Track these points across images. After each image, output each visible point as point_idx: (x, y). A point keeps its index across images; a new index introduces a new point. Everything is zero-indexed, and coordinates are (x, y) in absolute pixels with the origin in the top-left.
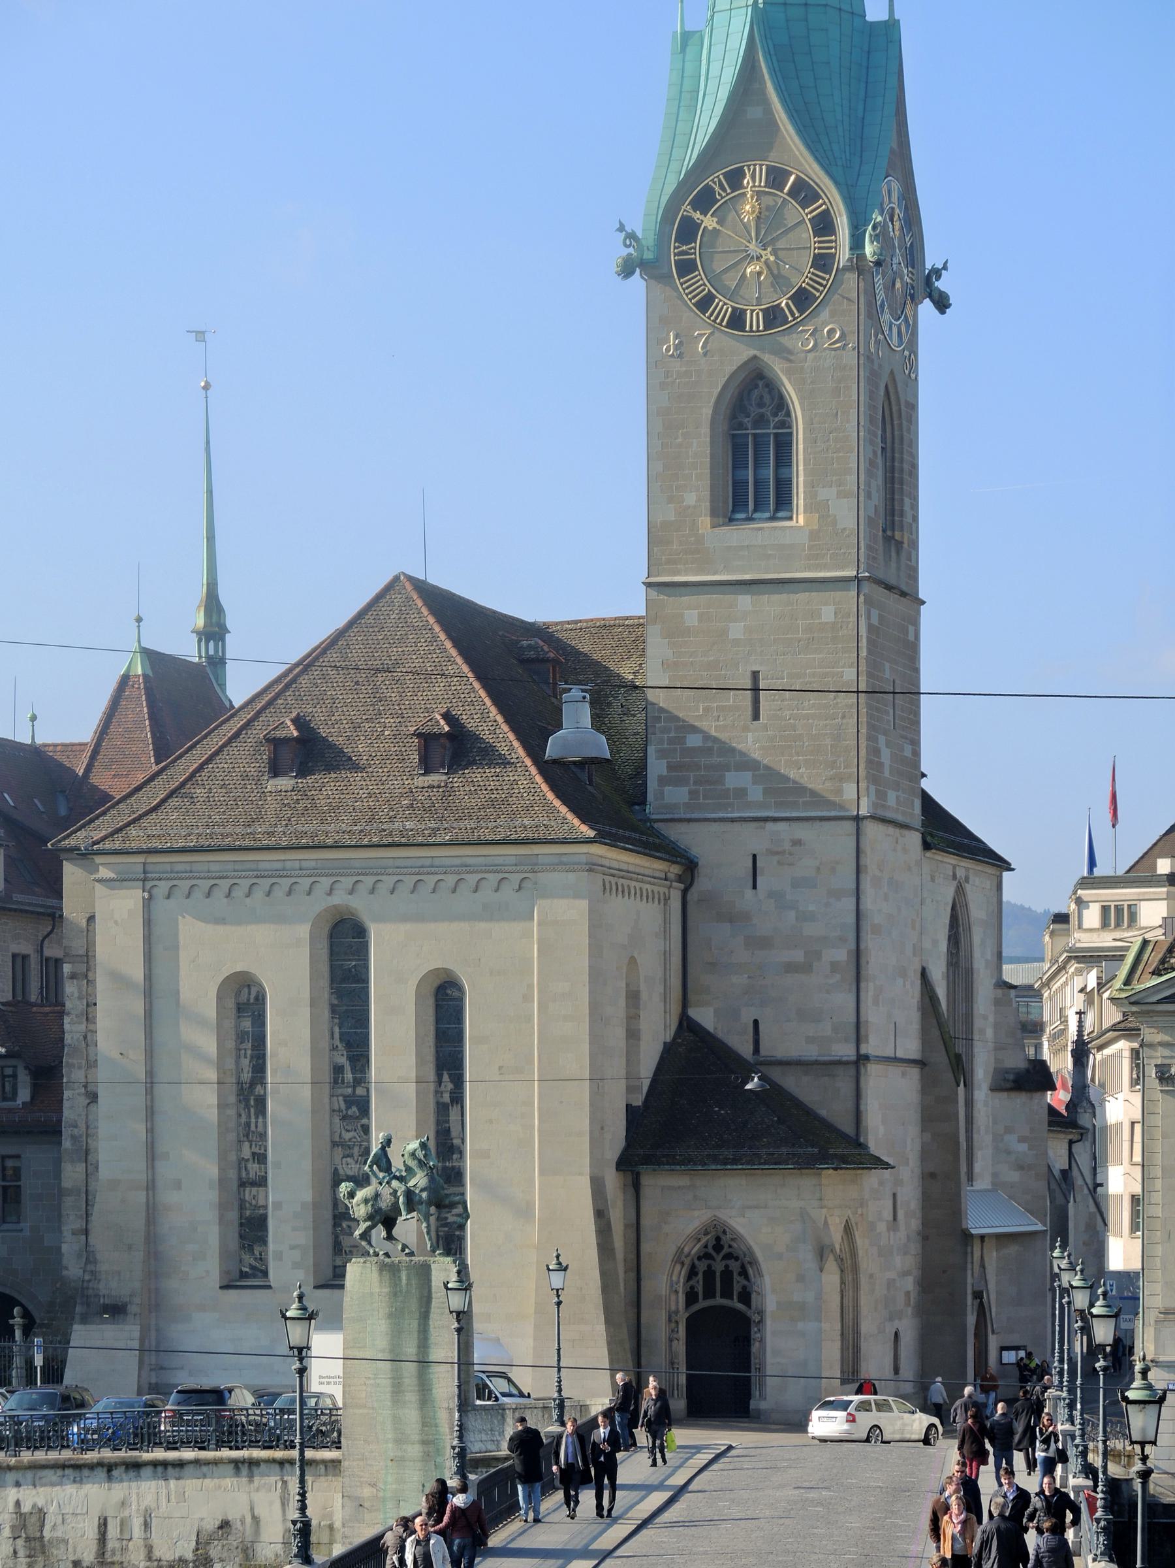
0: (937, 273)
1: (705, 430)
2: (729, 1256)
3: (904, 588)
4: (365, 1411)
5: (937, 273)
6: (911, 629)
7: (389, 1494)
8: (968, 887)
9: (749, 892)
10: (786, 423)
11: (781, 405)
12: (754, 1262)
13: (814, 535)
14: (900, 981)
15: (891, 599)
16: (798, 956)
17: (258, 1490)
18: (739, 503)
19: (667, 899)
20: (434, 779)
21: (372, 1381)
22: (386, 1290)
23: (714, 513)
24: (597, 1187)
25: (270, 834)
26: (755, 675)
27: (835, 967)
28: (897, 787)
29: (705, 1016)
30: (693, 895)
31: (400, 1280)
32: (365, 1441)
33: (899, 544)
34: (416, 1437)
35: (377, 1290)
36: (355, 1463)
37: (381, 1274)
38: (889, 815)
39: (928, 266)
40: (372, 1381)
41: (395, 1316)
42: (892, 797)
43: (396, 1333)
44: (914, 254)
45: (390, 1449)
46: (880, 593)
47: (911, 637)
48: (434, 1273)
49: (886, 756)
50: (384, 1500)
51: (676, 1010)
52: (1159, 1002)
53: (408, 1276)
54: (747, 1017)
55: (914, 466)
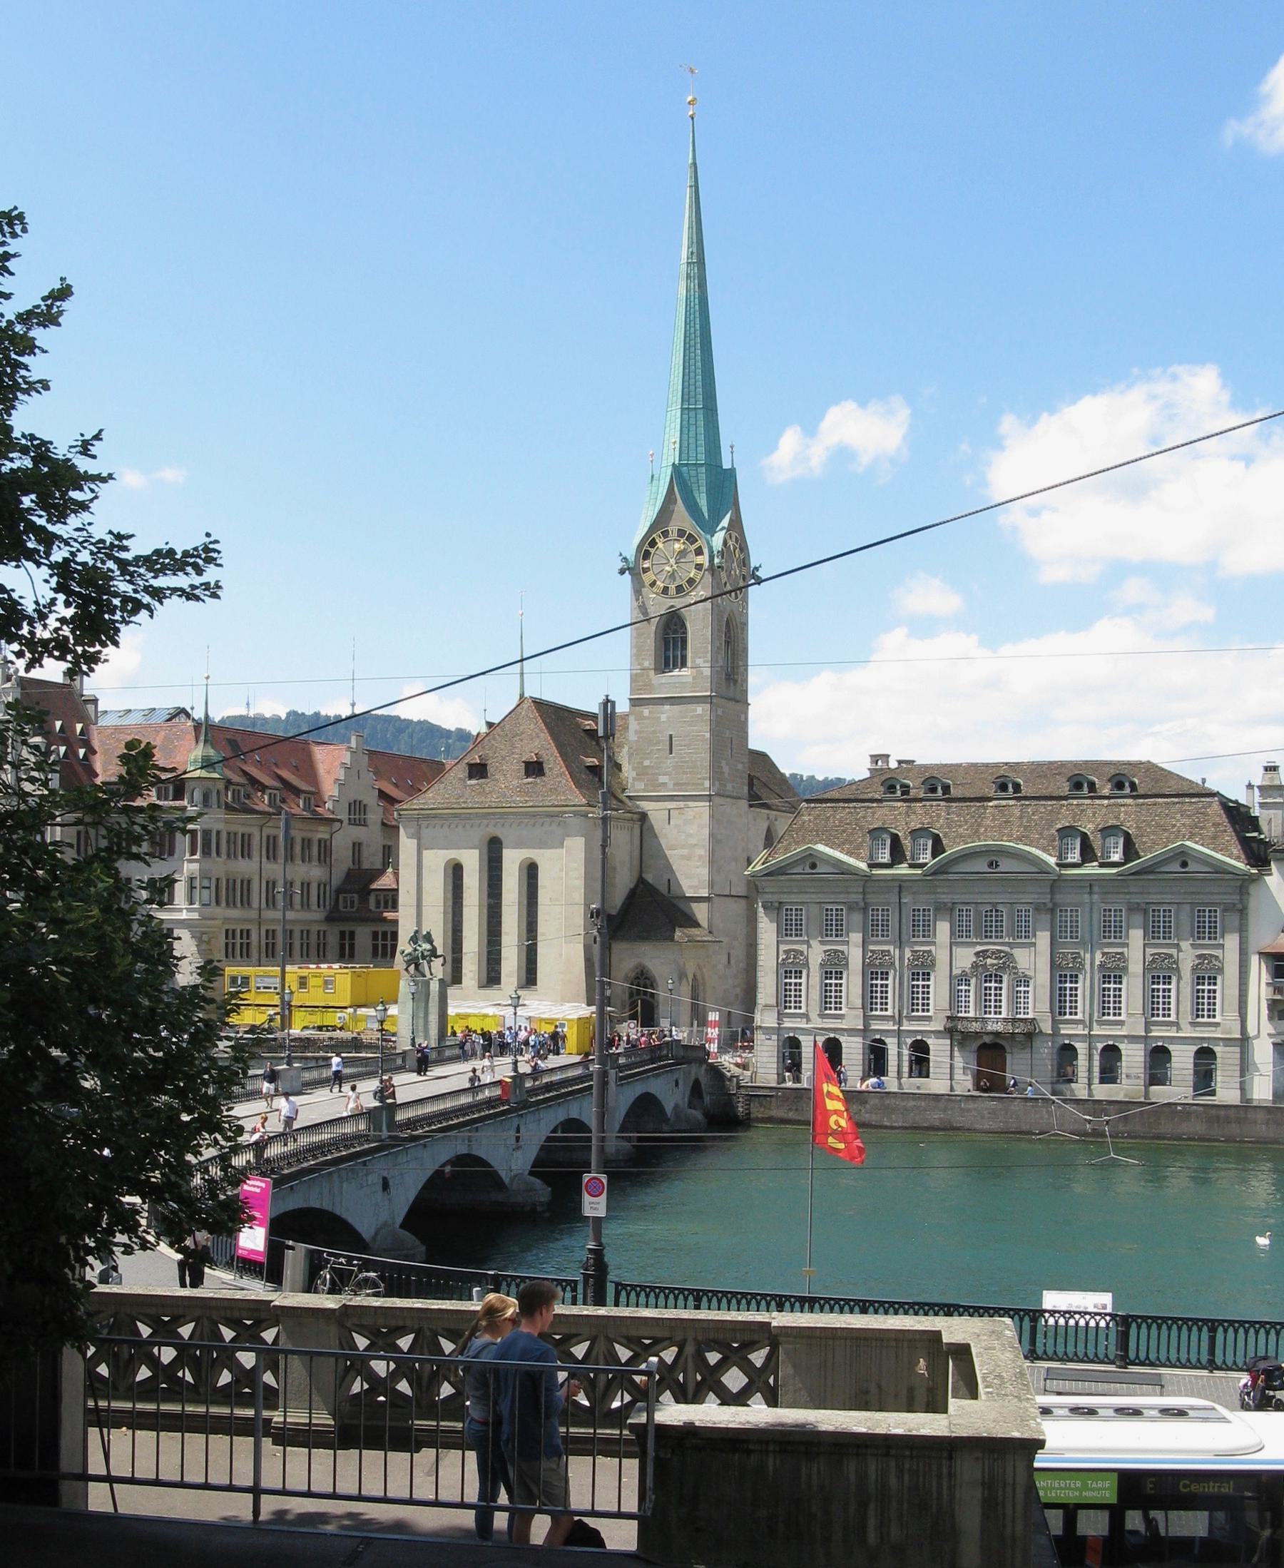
0: (757, 569)
1: (653, 635)
2: (646, 978)
3: (738, 698)
5: (757, 569)
6: (743, 716)
8: (777, 823)
9: (667, 826)
10: (685, 633)
11: (684, 626)
12: (655, 980)
13: (694, 678)
14: (734, 863)
15: (731, 704)
16: (685, 852)
18: (667, 664)
19: (632, 828)
20: (530, 780)
23: (655, 669)
24: (587, 949)
25: (465, 802)
26: (671, 736)
27: (700, 857)
28: (733, 781)
29: (649, 877)
30: (645, 827)
33: (736, 681)
38: (727, 793)
39: (753, 566)
42: (729, 787)
44: (745, 562)
46: (723, 702)
47: (743, 719)
49: (726, 769)
51: (636, 875)
54: (666, 877)
55: (745, 649)
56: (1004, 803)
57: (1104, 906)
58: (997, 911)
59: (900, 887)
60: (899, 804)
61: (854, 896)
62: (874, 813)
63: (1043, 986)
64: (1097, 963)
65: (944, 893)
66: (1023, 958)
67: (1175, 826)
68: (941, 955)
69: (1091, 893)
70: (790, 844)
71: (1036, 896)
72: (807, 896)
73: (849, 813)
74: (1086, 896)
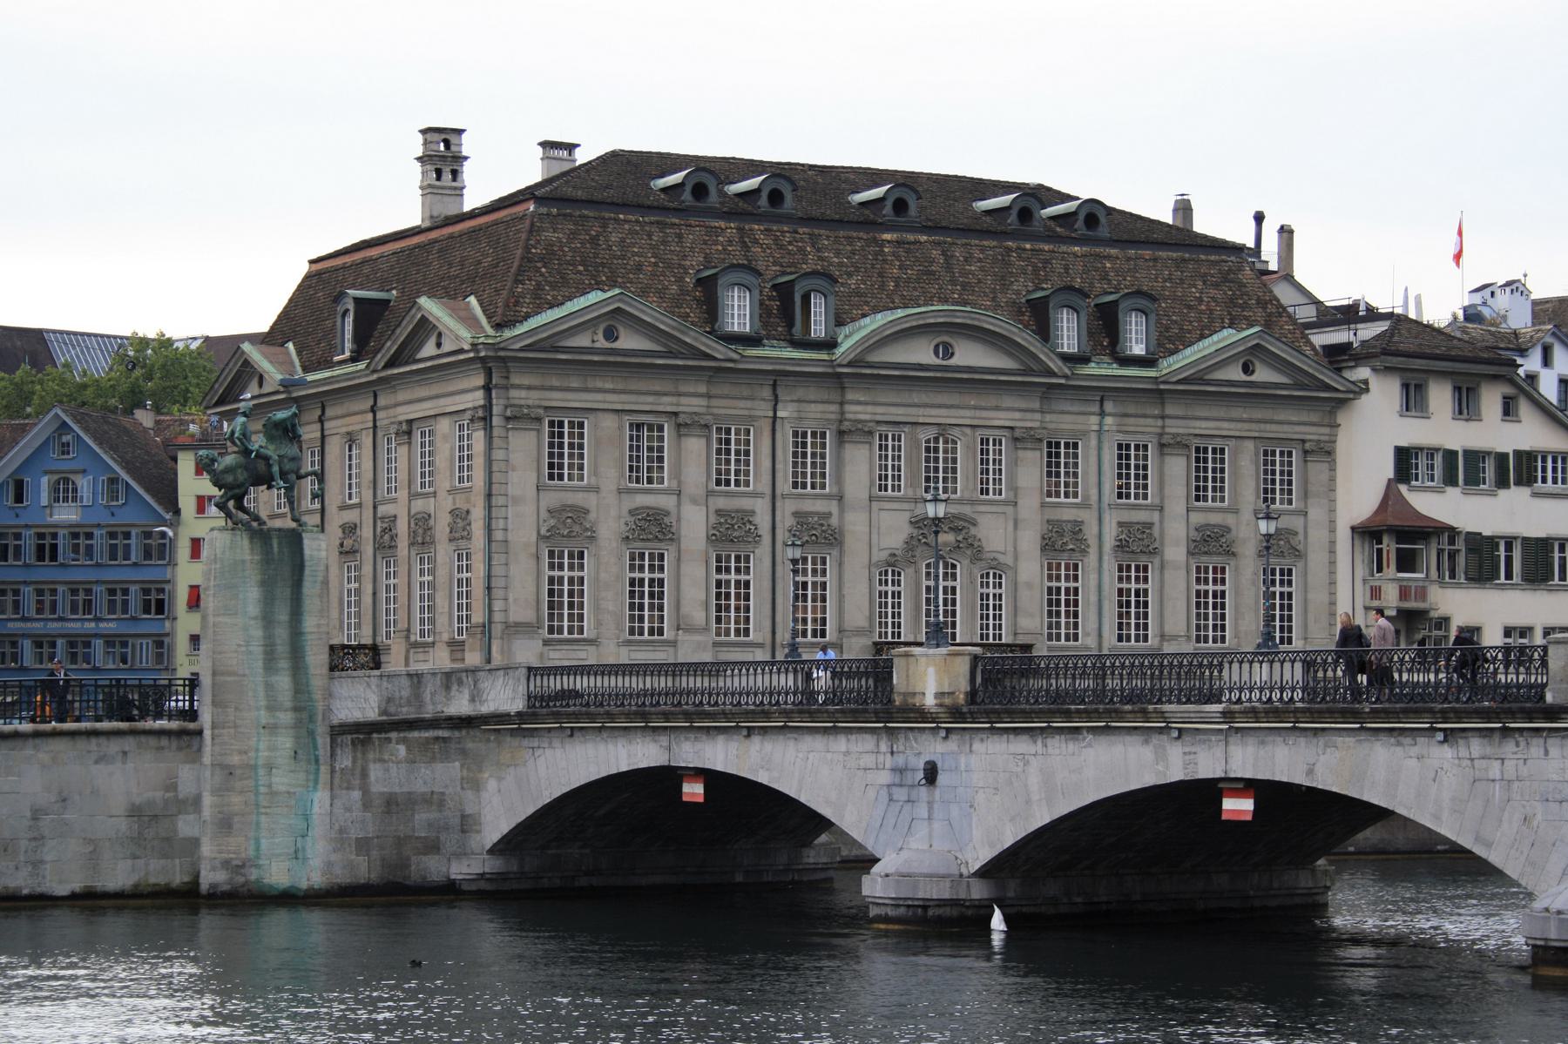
4: (236, 678)
7: (260, 762)
17: (96, 762)
21: (243, 649)
22: (257, 558)
31: (272, 548)
32: (236, 709)
34: (289, 704)
35: (248, 557)
36: (225, 731)
37: (251, 543)
40: (243, 649)
41: (267, 584)
43: (268, 601)
45: (264, 719)
48: (306, 542)
50: (255, 767)
52: (521, 350)
53: (280, 544)
56: (911, 237)
57: (1121, 437)
58: (946, 442)
59: (774, 386)
60: (722, 224)
61: (695, 401)
62: (680, 236)
63: (1029, 585)
64: (1109, 542)
65: (859, 403)
66: (993, 533)
67: (1200, 300)
68: (855, 524)
69: (1102, 414)
70: (539, 287)
71: (1017, 415)
72: (599, 397)
73: (632, 232)
74: (1094, 419)
